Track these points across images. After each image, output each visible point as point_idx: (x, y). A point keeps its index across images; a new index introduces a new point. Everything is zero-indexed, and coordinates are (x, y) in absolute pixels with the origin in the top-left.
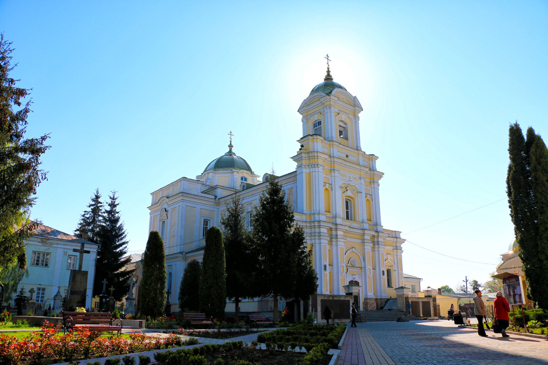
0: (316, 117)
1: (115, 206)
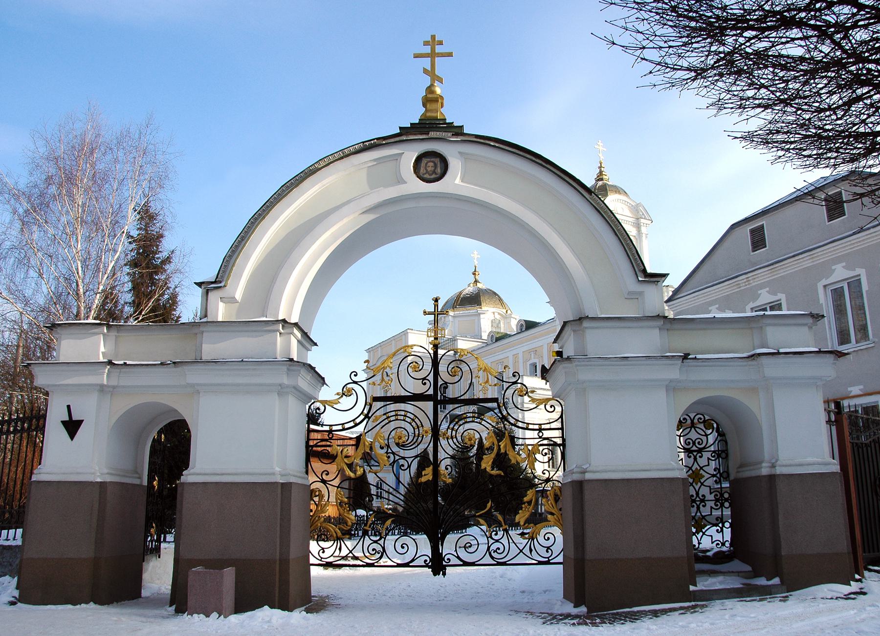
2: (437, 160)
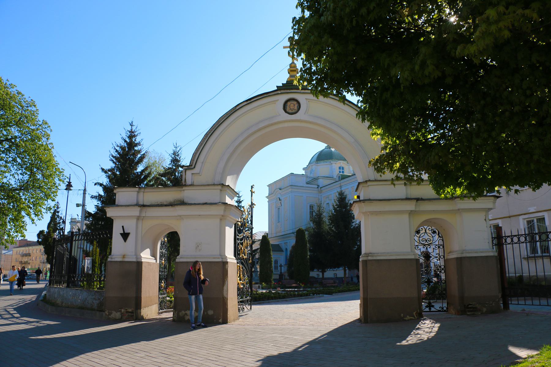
1: (241, 202)
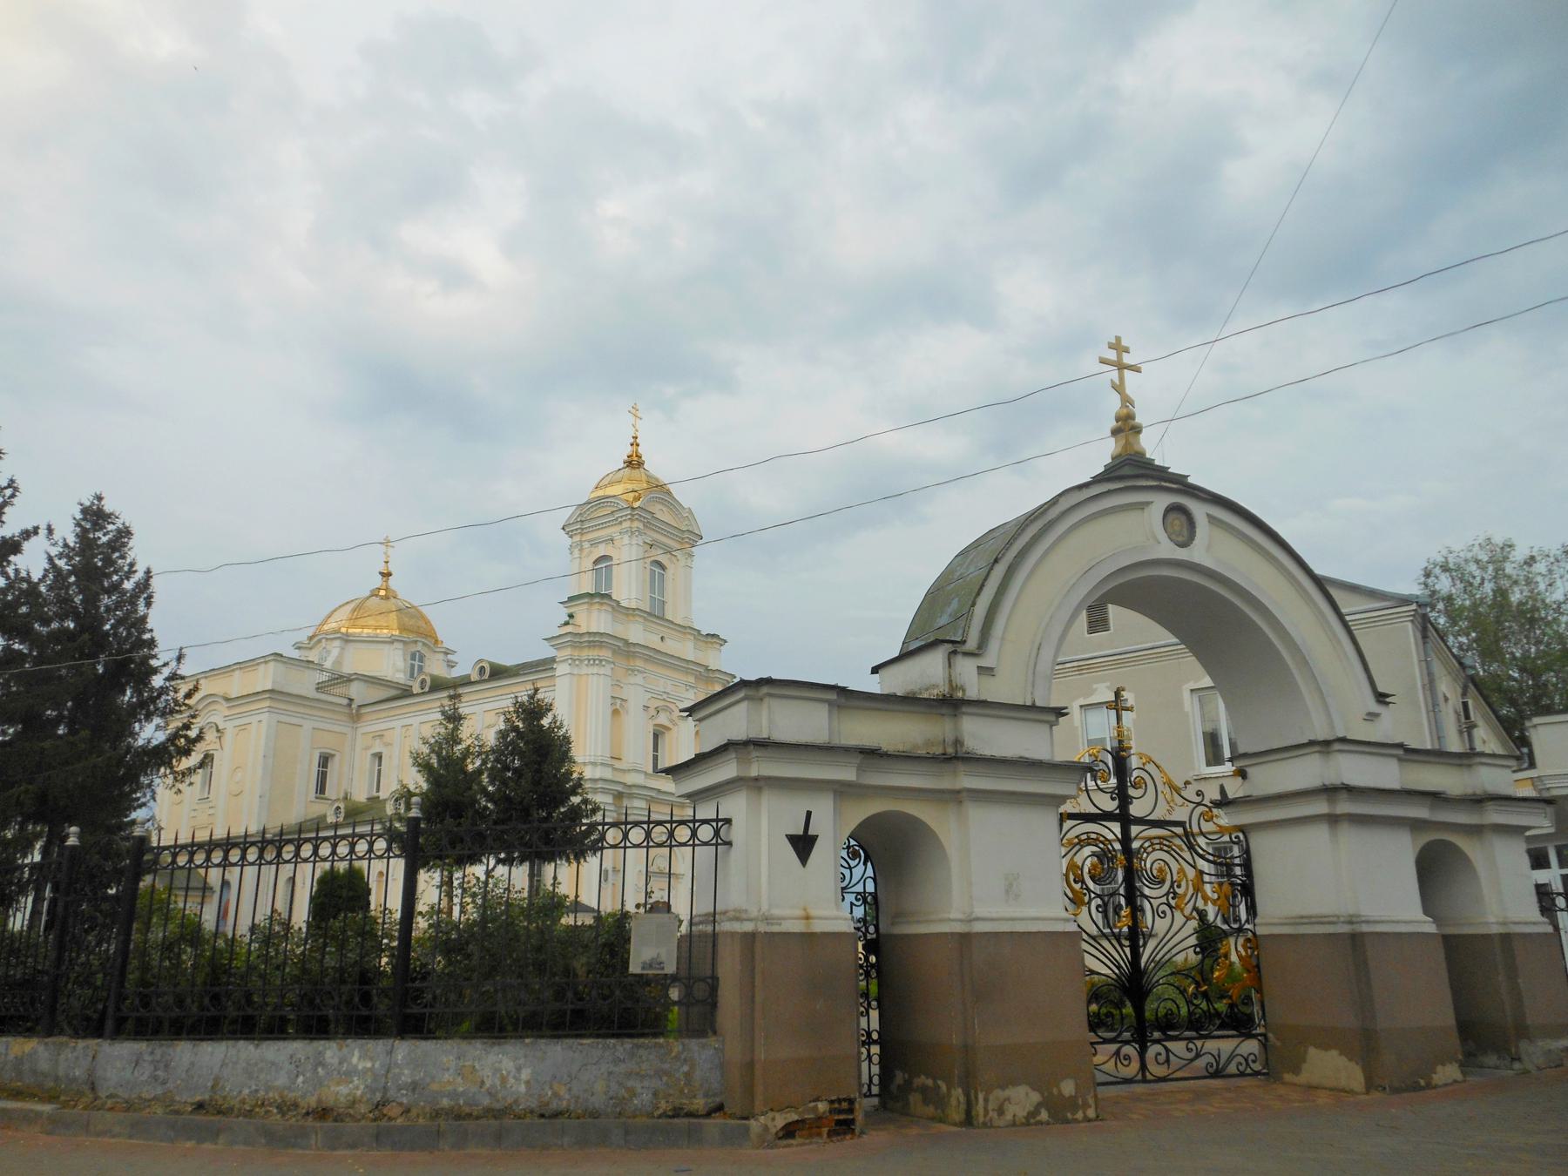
0: (601, 550)
2: (1183, 518)
